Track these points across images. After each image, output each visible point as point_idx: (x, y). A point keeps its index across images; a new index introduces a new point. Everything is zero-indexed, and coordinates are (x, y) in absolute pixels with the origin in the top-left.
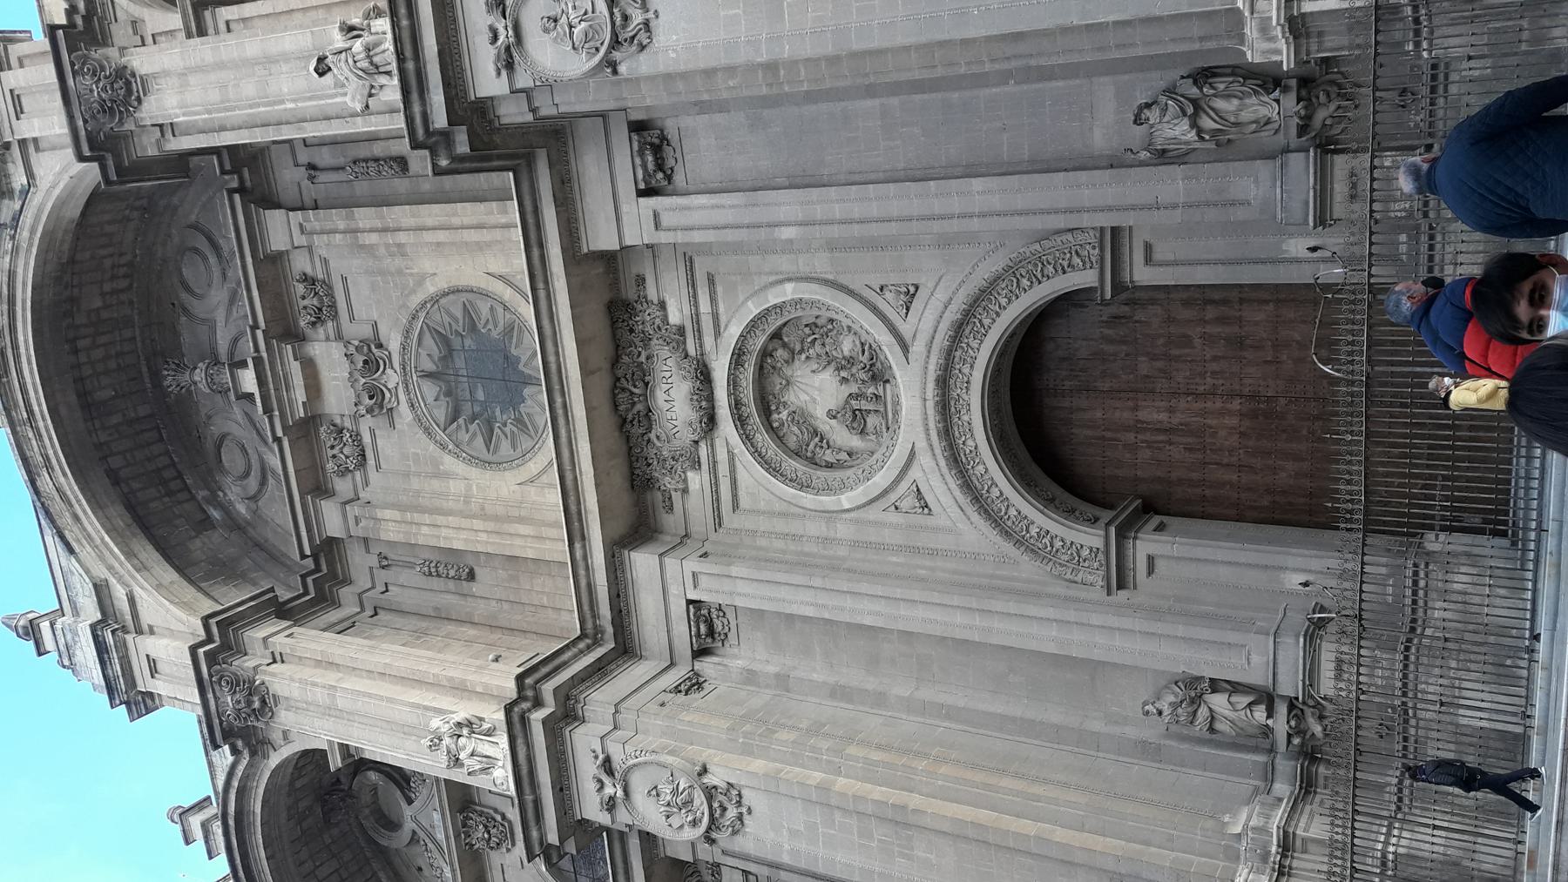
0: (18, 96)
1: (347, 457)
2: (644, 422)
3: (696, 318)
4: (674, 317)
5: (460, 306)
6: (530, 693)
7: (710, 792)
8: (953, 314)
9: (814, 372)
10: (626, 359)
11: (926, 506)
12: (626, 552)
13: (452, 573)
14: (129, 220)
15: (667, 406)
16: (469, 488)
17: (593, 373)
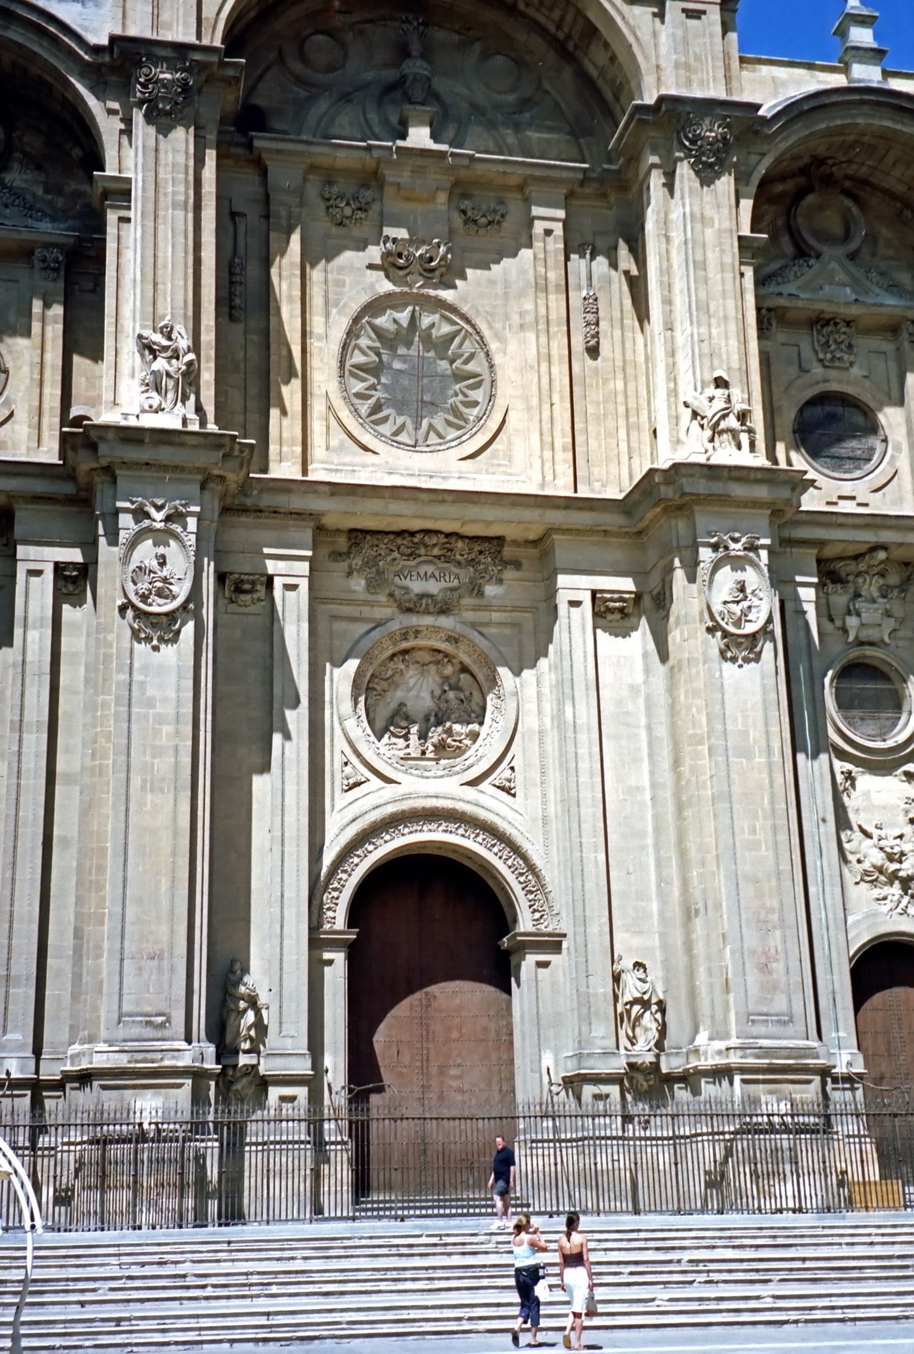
0: (699, 18)
1: (342, 208)
2: (409, 551)
3: (487, 608)
4: (490, 590)
5: (478, 370)
6: (236, 453)
7: (171, 616)
8: (502, 825)
9: (432, 692)
10: (460, 544)
11: (350, 789)
12: (312, 524)
13: (237, 301)
14: (559, 27)
15: (422, 574)
16: (319, 339)
17: (462, 525)
